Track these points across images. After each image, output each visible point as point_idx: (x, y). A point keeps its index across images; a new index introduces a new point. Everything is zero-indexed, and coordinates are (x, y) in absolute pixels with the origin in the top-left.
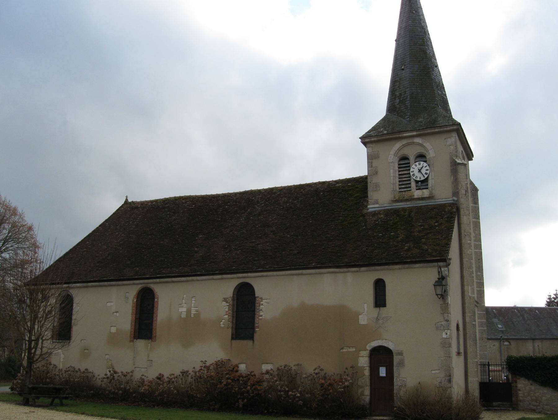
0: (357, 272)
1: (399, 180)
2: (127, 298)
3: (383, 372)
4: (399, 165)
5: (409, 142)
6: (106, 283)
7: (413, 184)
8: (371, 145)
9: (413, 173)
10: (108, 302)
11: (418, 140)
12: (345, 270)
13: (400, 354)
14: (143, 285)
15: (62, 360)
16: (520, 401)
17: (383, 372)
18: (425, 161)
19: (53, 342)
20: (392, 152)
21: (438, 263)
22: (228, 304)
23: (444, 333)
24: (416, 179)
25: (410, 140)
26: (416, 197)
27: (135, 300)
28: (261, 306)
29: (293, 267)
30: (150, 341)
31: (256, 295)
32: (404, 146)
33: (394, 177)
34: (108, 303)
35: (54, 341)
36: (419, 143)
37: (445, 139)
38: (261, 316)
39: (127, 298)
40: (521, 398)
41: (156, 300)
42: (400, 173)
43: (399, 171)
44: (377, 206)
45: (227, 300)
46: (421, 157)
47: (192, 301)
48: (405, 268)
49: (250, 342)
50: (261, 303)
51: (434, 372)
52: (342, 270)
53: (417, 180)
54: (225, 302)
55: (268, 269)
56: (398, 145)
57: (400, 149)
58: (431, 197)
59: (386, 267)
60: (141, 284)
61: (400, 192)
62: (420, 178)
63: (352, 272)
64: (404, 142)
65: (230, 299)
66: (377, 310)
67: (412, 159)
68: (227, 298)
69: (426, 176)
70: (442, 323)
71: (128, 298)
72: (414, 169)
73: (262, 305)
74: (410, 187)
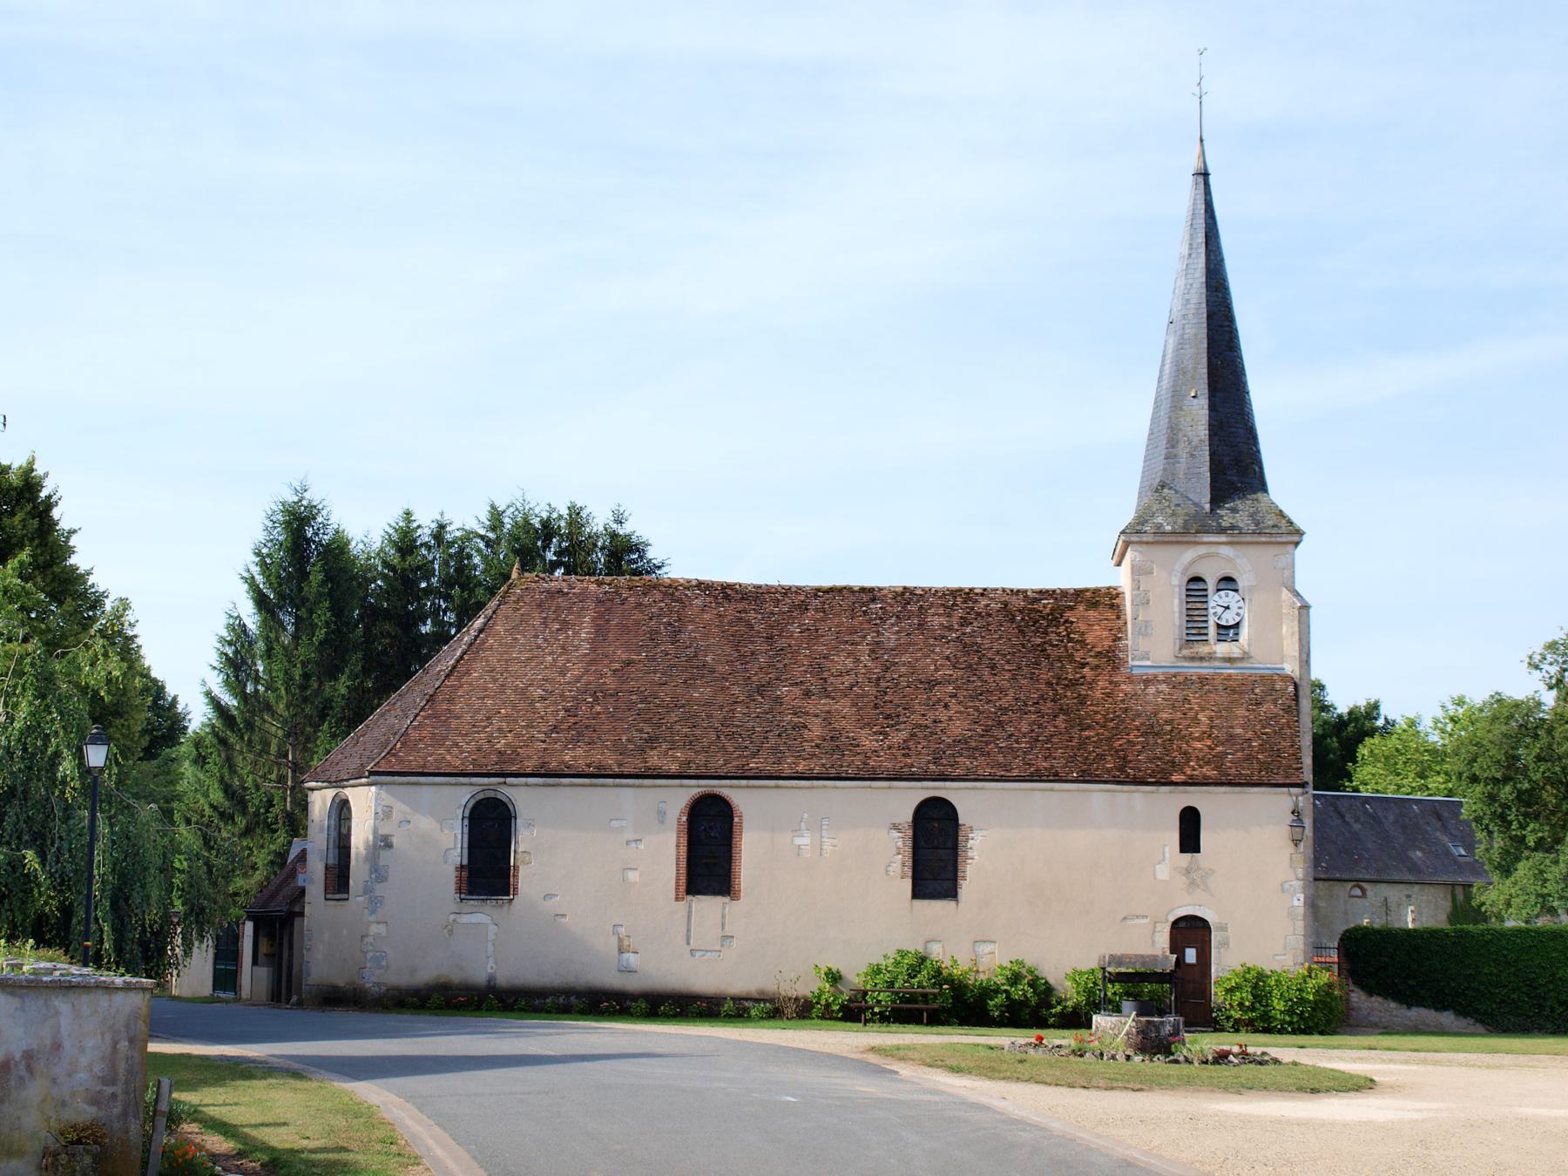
0: (1153, 792)
1: (1187, 619)
2: (661, 814)
3: (1191, 955)
4: (1187, 590)
5: (1210, 551)
6: (610, 781)
7: (1212, 631)
8: (1140, 548)
9: (1215, 610)
10: (611, 820)
11: (1226, 551)
12: (1133, 788)
13: (1223, 928)
14: (702, 789)
15: (491, 937)
16: (1353, 1009)
17: (1191, 955)
18: (1236, 591)
19: (461, 899)
20: (1179, 567)
21: (1291, 789)
22: (900, 834)
23: (1295, 899)
24: (1219, 622)
25: (1212, 549)
26: (1219, 655)
27: (684, 819)
28: (970, 841)
29: (1038, 778)
30: (726, 899)
31: (960, 822)
32: (1201, 557)
33: (1180, 612)
34: (614, 822)
35: (463, 896)
36: (1228, 556)
37: (1275, 556)
38: (972, 859)
39: (661, 814)
40: (1355, 1005)
41: (736, 820)
42: (1189, 607)
43: (1187, 602)
44: (1148, 663)
45: (900, 827)
46: (1228, 582)
47: (821, 825)
48: (1233, 793)
49: (952, 904)
50: (970, 835)
51: (1278, 958)
52: (1125, 788)
53: (1222, 623)
54: (894, 831)
55: (987, 777)
56: (1189, 554)
57: (1193, 562)
58: (1245, 657)
59: (1204, 788)
60: (699, 786)
61: (1187, 641)
62: (1227, 621)
63: (1143, 792)
64: (1202, 550)
65: (906, 825)
66: (1188, 856)
67: (1211, 585)
68: (899, 824)
69: (1238, 619)
70: (1294, 883)
71: (665, 813)
72: (1216, 600)
73: (973, 839)
74: (1206, 634)
